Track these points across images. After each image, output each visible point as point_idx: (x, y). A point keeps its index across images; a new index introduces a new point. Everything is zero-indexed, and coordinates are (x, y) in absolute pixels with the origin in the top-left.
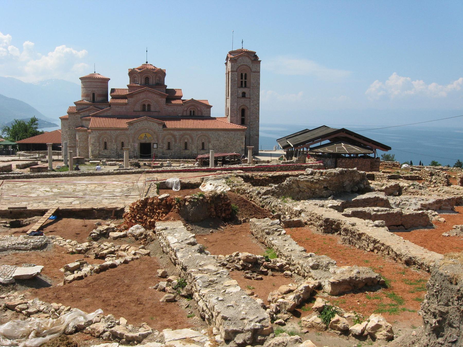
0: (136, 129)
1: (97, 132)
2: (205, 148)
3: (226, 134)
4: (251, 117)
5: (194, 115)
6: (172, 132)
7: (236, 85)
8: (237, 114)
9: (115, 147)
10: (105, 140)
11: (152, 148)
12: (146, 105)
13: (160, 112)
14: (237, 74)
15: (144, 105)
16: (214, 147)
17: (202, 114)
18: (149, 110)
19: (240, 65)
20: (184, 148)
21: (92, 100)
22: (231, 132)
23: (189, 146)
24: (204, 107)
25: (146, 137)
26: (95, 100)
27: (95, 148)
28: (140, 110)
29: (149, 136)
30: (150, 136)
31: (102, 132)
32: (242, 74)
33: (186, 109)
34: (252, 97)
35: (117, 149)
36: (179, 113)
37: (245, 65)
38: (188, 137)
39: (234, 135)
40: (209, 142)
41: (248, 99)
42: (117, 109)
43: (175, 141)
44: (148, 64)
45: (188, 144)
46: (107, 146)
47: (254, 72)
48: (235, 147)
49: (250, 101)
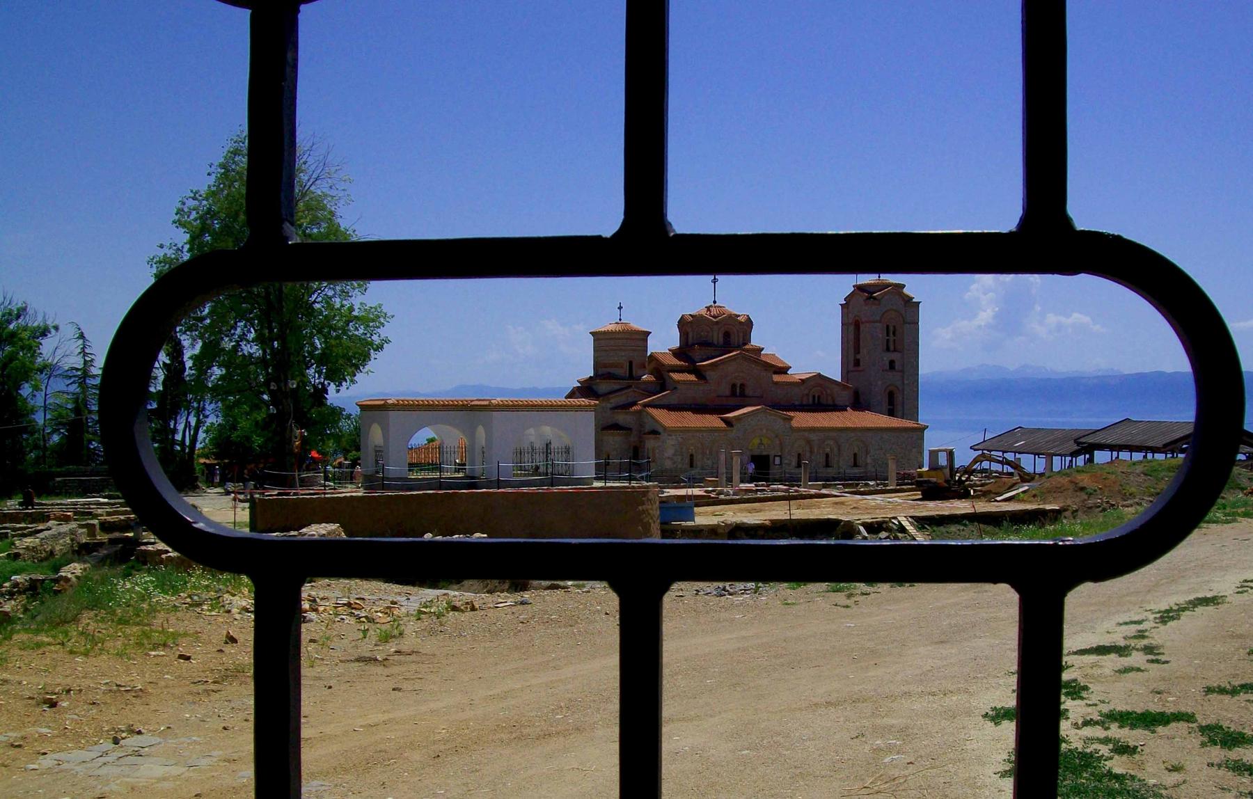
2: (860, 462)
6: (806, 434)
12: (739, 385)
15: (734, 386)
17: (834, 401)
18: (743, 395)
20: (824, 464)
21: (628, 375)
25: (761, 444)
29: (765, 441)
30: (769, 442)
32: (888, 327)
33: (806, 392)
37: (895, 311)
40: (867, 452)
43: (811, 452)
47: (909, 323)
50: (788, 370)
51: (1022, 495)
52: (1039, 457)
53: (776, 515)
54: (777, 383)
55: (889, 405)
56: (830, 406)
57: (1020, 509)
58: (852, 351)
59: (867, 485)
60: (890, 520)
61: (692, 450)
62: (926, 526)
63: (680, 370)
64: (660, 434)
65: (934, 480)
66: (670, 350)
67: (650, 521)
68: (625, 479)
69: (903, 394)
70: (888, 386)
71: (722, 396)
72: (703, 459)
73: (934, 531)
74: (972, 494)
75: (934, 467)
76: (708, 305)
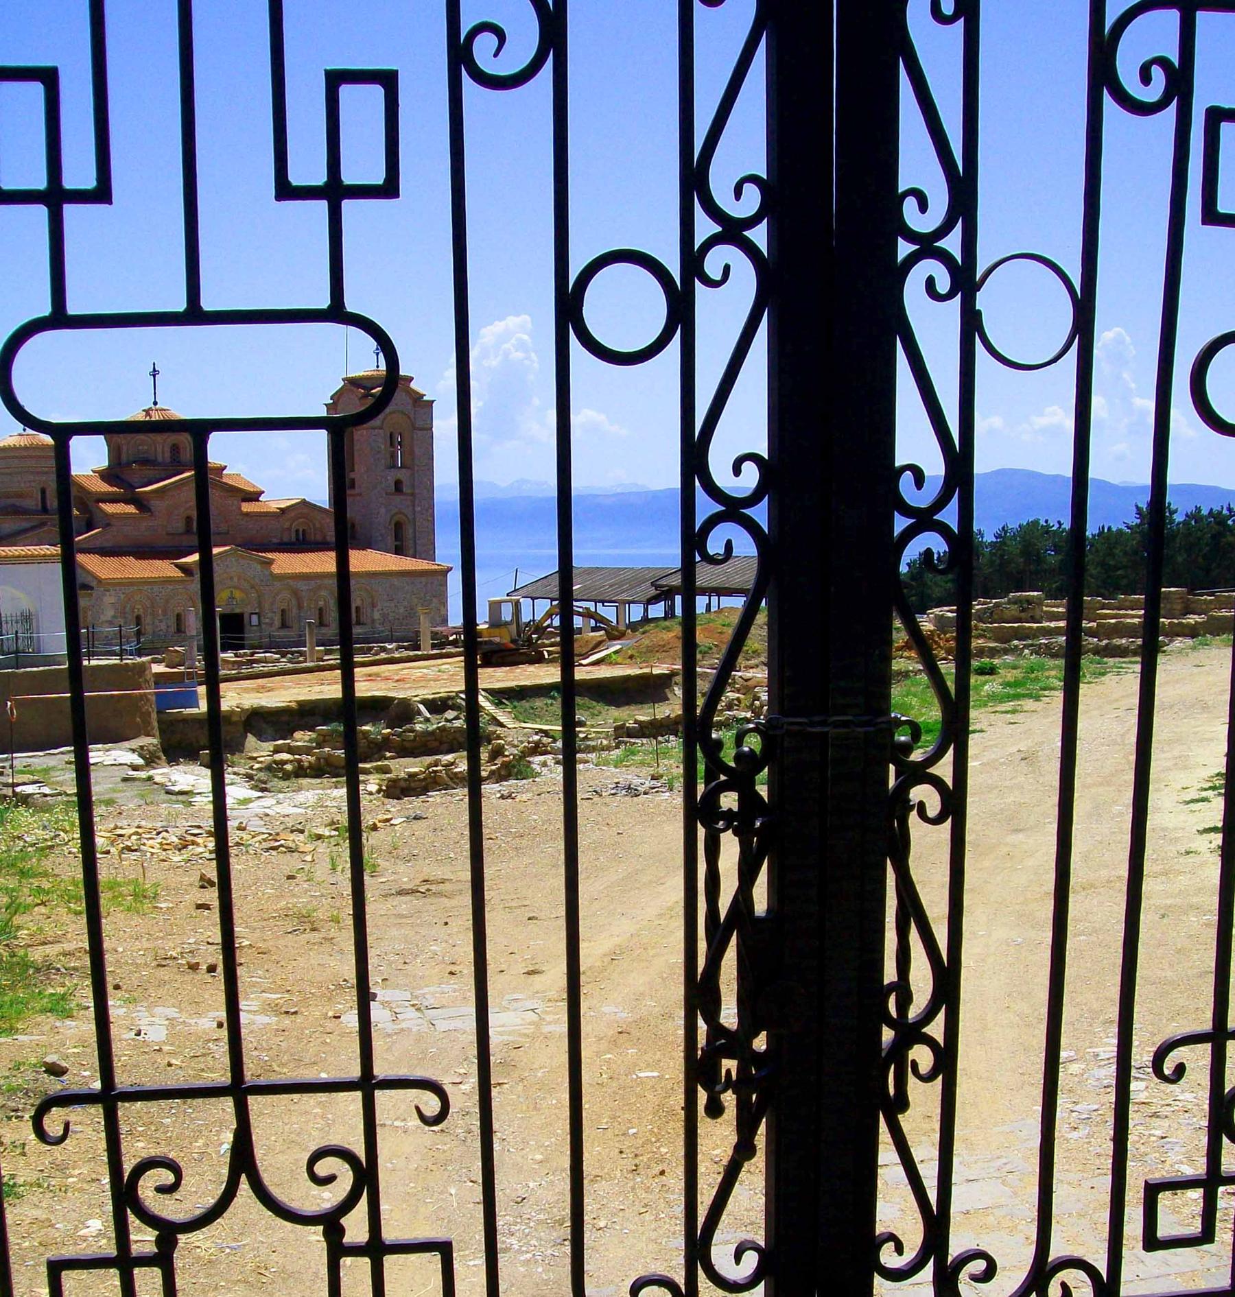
9: (163, 626)
10: (139, 610)
11: (247, 628)
13: (228, 533)
14: (383, 435)
16: (385, 616)
17: (324, 538)
26: (49, 507)
29: (237, 594)
30: (243, 595)
33: (287, 525)
40: (373, 606)
43: (300, 607)
44: (157, 406)
51: (614, 657)
52: (603, 606)
53: (298, 694)
54: (247, 514)
55: (396, 539)
56: (317, 543)
57: (621, 674)
59: (384, 650)
60: (457, 695)
61: (138, 609)
62: (504, 700)
63: (113, 499)
64: (91, 588)
65: (497, 640)
66: (94, 472)
67: (150, 709)
68: (113, 654)
70: (392, 516)
73: (515, 707)
74: (546, 657)
75: (496, 623)
76: (146, 408)
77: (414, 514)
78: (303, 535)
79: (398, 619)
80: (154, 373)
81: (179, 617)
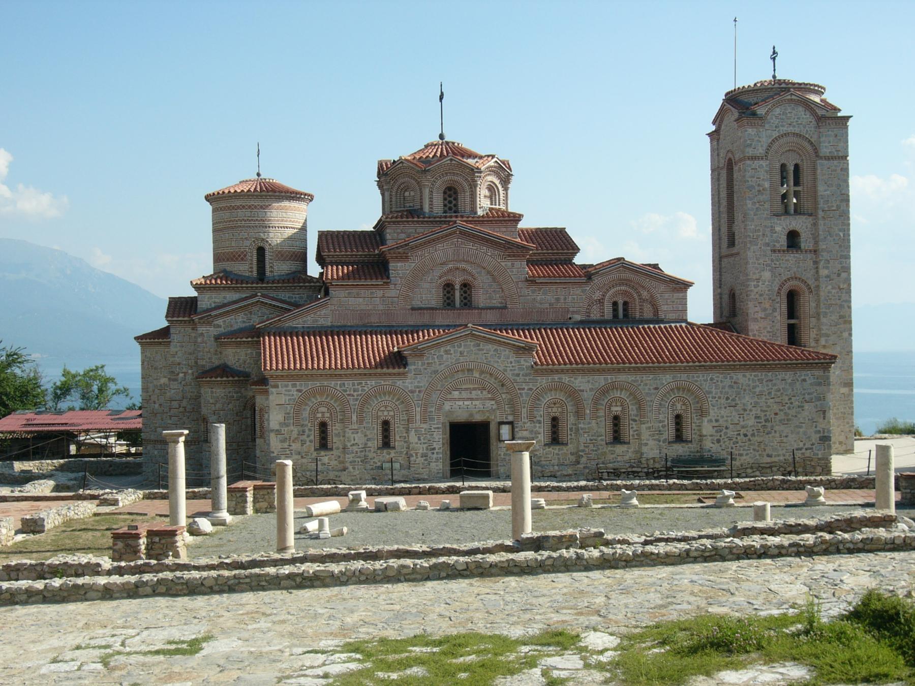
0: (436, 372)
1: (294, 386)
2: (687, 433)
3: (761, 381)
4: (824, 320)
5: (626, 315)
6: (566, 379)
7: (767, 206)
8: (774, 310)
9: (359, 438)
10: (323, 414)
11: (493, 441)
12: (457, 287)
15: (448, 287)
17: (656, 311)
18: (467, 303)
19: (775, 134)
20: (610, 438)
21: (255, 274)
22: (782, 375)
23: (629, 430)
24: (662, 287)
26: (268, 273)
27: (286, 445)
28: (433, 304)
31: (311, 384)
33: (598, 295)
34: (822, 246)
35: (365, 446)
36: (577, 312)
38: (624, 395)
39: (790, 384)
40: (702, 413)
41: (809, 256)
42: (352, 301)
43: (579, 414)
45: (624, 422)
46: (329, 438)
47: (828, 158)
48: (798, 427)
49: (816, 263)
50: (574, 254)
55: (788, 319)
58: (725, 216)
61: (323, 413)
69: (818, 295)
70: (786, 281)
71: (420, 309)
72: (344, 432)
77: (817, 279)
78: (625, 310)
79: (745, 435)
80: (441, 98)
81: (386, 424)
